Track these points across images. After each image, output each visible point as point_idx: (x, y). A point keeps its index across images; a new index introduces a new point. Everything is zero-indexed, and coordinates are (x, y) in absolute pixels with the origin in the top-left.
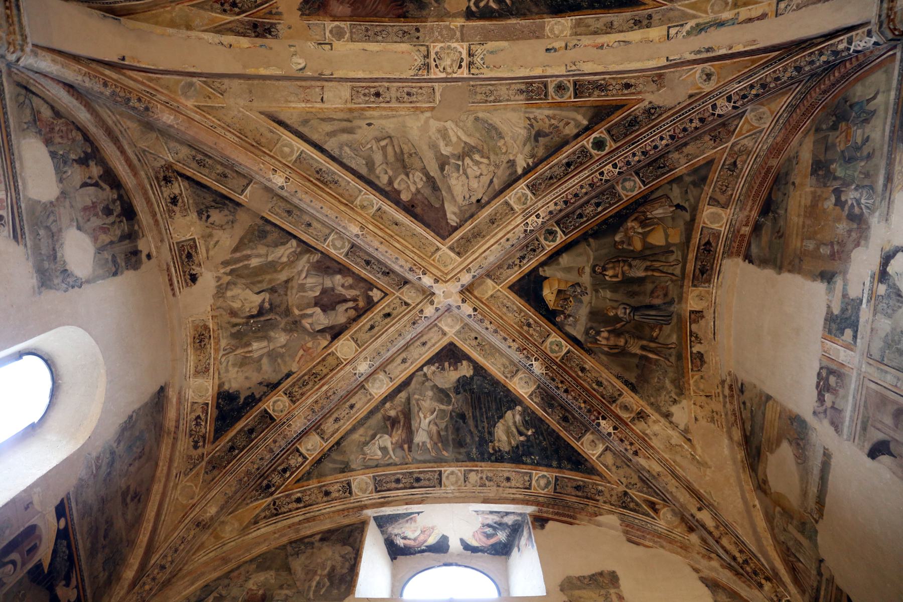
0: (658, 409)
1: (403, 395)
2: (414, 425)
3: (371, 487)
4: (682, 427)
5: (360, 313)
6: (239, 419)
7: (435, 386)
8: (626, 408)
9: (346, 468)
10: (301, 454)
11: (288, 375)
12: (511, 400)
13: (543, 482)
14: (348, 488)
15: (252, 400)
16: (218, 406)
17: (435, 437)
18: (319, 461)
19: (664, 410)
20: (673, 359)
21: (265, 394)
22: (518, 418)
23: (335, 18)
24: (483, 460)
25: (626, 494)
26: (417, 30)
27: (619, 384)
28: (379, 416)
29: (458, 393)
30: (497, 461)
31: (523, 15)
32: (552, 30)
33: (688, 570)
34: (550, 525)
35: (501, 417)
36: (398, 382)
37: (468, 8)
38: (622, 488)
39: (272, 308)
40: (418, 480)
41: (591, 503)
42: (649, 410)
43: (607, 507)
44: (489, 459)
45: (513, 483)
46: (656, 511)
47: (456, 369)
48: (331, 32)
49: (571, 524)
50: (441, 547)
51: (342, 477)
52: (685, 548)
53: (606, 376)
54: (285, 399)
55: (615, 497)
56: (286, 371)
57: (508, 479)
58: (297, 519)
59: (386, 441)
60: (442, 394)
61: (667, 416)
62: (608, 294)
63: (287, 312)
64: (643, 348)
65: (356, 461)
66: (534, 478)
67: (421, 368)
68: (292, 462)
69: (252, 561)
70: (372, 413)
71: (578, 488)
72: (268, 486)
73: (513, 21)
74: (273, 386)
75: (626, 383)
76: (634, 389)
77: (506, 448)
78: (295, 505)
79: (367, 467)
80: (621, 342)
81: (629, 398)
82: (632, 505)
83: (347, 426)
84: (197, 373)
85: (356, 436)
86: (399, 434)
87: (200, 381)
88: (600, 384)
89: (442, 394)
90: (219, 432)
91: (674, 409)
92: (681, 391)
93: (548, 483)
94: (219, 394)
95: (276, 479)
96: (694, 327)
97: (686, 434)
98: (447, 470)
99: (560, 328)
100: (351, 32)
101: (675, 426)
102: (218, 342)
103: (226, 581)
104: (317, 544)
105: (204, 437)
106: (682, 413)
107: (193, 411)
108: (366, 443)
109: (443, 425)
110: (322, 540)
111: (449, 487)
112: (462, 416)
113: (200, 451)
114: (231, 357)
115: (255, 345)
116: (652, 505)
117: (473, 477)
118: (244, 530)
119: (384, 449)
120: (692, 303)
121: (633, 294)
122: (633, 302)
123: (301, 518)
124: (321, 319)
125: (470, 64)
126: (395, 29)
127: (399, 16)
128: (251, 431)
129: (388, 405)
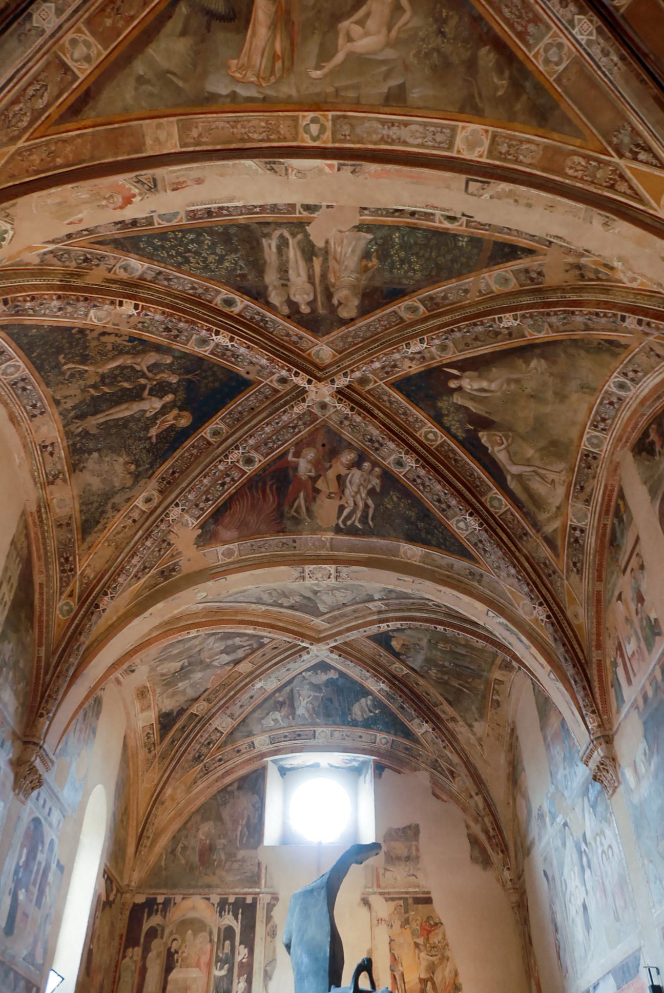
0: (465, 720)
1: (288, 688)
2: (296, 704)
3: (268, 741)
4: (478, 735)
5: (254, 651)
6: (175, 724)
7: (311, 683)
8: (444, 712)
9: (250, 734)
10: (219, 731)
11: (205, 691)
12: (366, 692)
13: (384, 741)
14: (252, 745)
15: (182, 711)
16: (160, 722)
17: (311, 711)
18: (232, 733)
19: (469, 722)
20: (479, 697)
21: (190, 705)
22: (369, 702)
23: (225, 543)
24: (344, 725)
25: (436, 761)
26: (294, 541)
27: (441, 698)
28: (271, 701)
29: (327, 686)
30: (353, 725)
31: (383, 537)
32: (405, 553)
33: (463, 825)
34: (387, 773)
35: (358, 700)
36: (284, 681)
37: (337, 525)
38: (435, 757)
39: (190, 664)
40: (299, 735)
41: (414, 760)
42: (459, 718)
43: (423, 765)
44: (348, 724)
45: (364, 739)
46: (453, 777)
47: (326, 674)
48: (223, 554)
49: (399, 772)
50: (316, 766)
51: (248, 740)
52: (464, 810)
53: (432, 691)
54: (205, 704)
55: (429, 762)
56: (203, 690)
57: (361, 737)
58: (220, 773)
59: (278, 715)
60: (316, 687)
61: (470, 726)
62: (439, 654)
63: (201, 662)
64: (460, 685)
65: (256, 729)
66: (378, 738)
67: (301, 673)
68: (213, 737)
69: (198, 811)
70: (266, 700)
71: (406, 749)
72: (199, 757)
73: (374, 540)
74: (196, 700)
75: (446, 699)
76: (450, 703)
77: (360, 719)
78: (218, 764)
79: (264, 732)
80: (446, 677)
81: (446, 707)
82: (439, 769)
83: (250, 709)
84: (142, 710)
85: (256, 715)
86: (285, 710)
87: (146, 714)
88: (428, 694)
89: (316, 687)
90: (162, 737)
91: (475, 724)
92: (482, 715)
93: (388, 742)
94: (160, 716)
95: (204, 750)
96: (496, 686)
97: (480, 740)
98: (319, 730)
99: (403, 662)
100: (239, 550)
101: (474, 734)
102: (154, 691)
103: (185, 832)
104: (236, 793)
105: (154, 744)
106: (480, 727)
107: (143, 731)
108: (263, 718)
109: (316, 704)
110: (239, 788)
111: (320, 741)
112: (331, 700)
113: (153, 753)
114: (165, 695)
115: (180, 684)
116: (452, 773)
117: (337, 734)
118: (189, 790)
119: (276, 720)
120: (497, 675)
121: (457, 659)
122: (456, 662)
123: (224, 771)
124: (226, 658)
125: (337, 578)
126: (275, 542)
127: (278, 532)
128: (184, 727)
129: (277, 695)
